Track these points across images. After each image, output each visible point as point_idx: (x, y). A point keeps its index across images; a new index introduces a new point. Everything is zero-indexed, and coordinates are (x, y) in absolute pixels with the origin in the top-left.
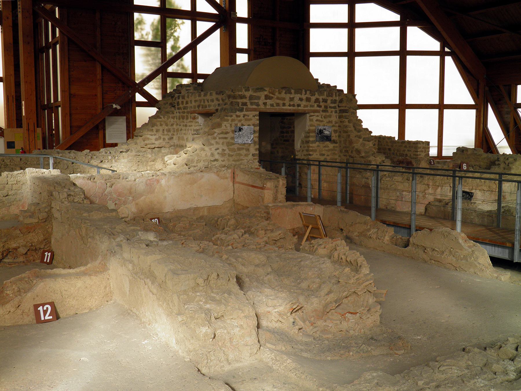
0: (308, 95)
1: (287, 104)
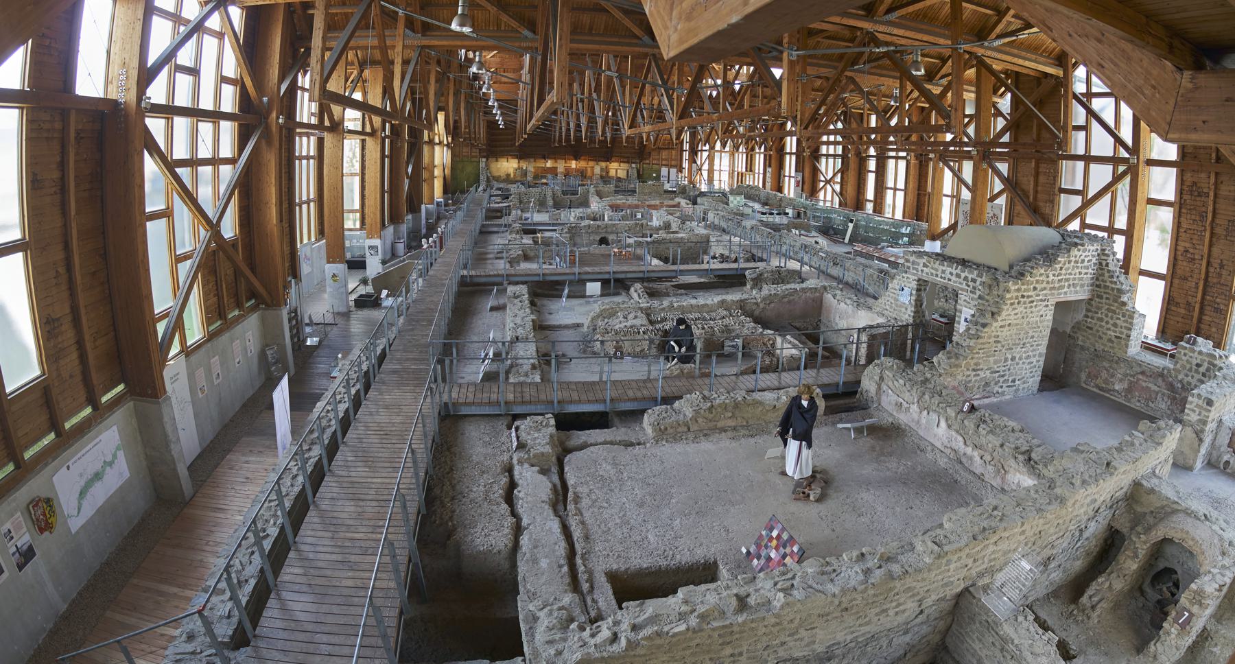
0: (958, 271)
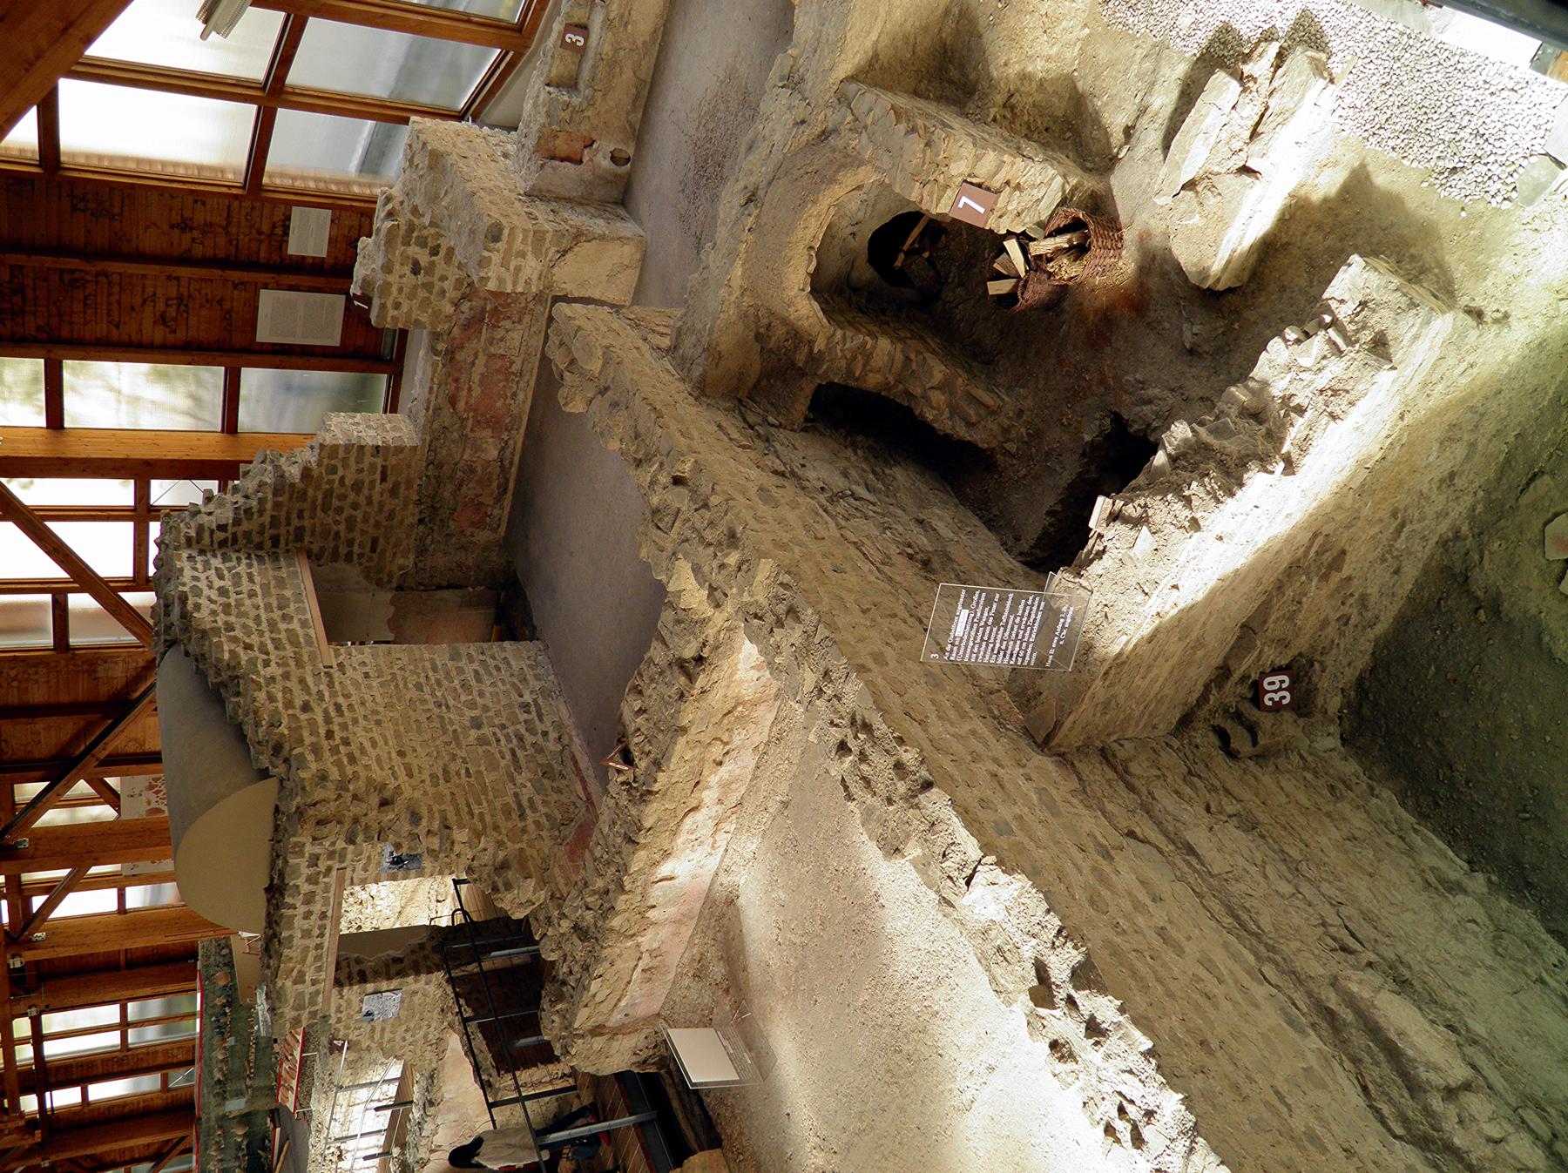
1: (318, 941)
